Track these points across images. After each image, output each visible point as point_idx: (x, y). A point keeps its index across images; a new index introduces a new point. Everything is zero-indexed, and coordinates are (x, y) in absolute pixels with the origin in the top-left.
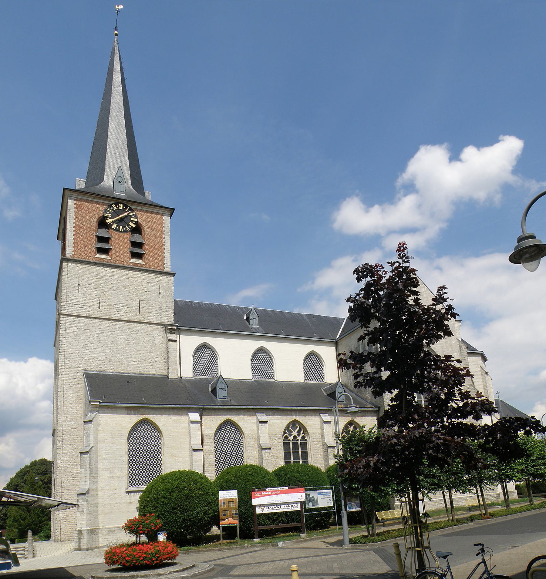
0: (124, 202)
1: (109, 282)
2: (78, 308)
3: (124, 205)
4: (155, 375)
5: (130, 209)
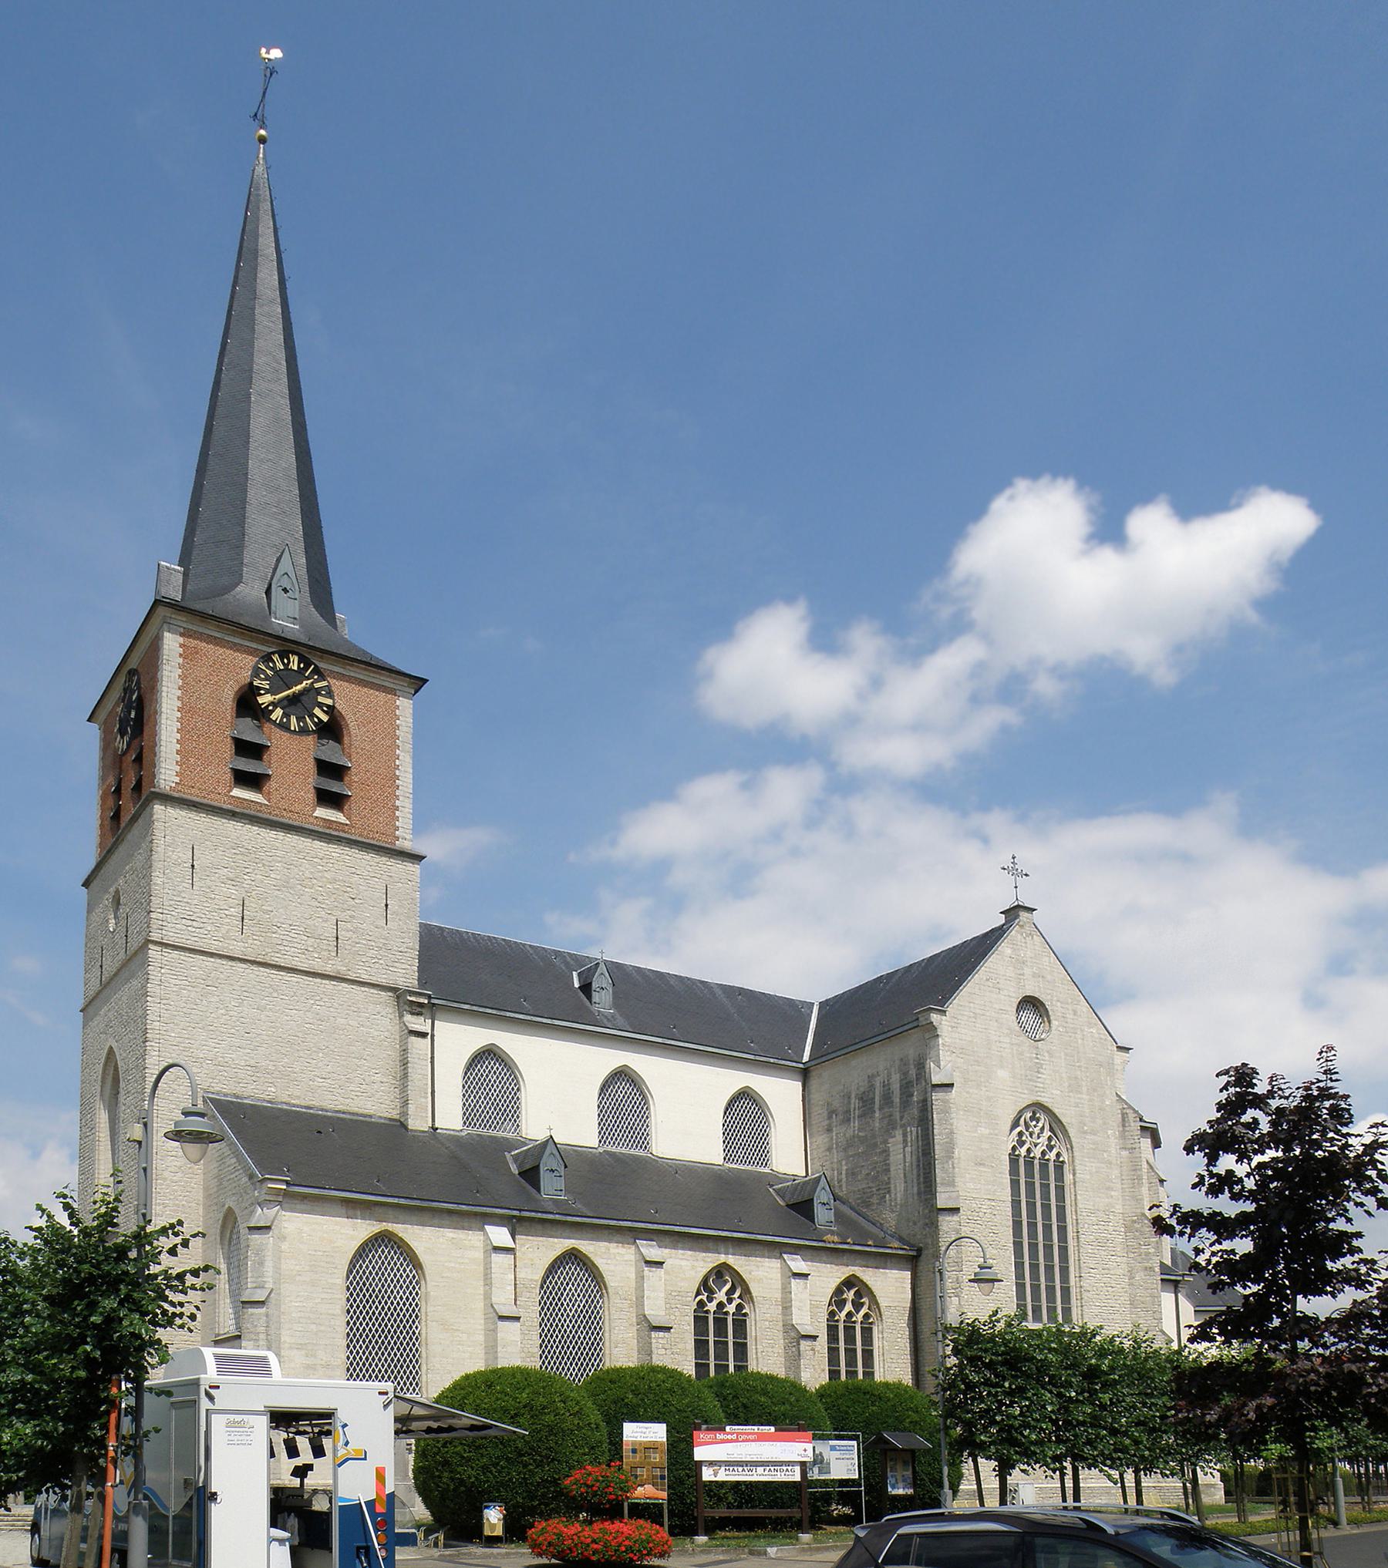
0: (302, 650)
1: (264, 865)
2: (189, 928)
5: (317, 671)
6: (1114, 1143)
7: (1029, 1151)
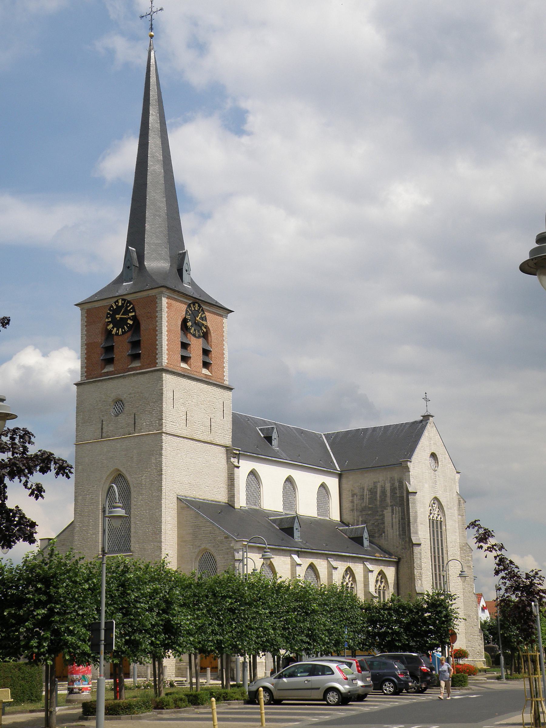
4: (220, 502)
6: (456, 512)
7: (433, 517)
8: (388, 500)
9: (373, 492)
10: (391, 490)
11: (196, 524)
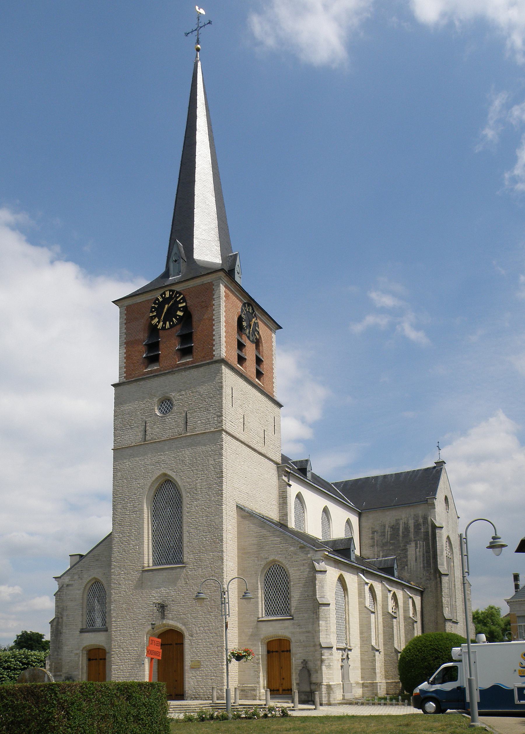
3: (253, 309)
5: (255, 315)
8: (412, 536)
9: (395, 528)
10: (414, 526)
11: (261, 534)
